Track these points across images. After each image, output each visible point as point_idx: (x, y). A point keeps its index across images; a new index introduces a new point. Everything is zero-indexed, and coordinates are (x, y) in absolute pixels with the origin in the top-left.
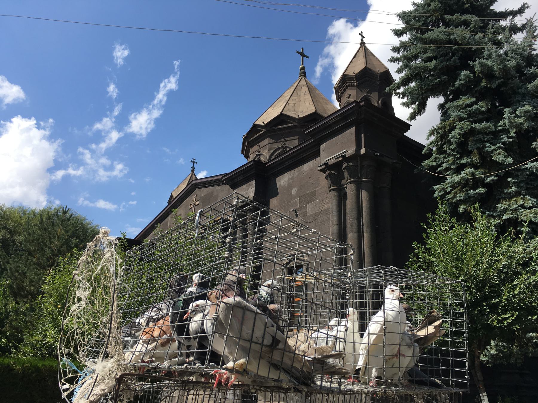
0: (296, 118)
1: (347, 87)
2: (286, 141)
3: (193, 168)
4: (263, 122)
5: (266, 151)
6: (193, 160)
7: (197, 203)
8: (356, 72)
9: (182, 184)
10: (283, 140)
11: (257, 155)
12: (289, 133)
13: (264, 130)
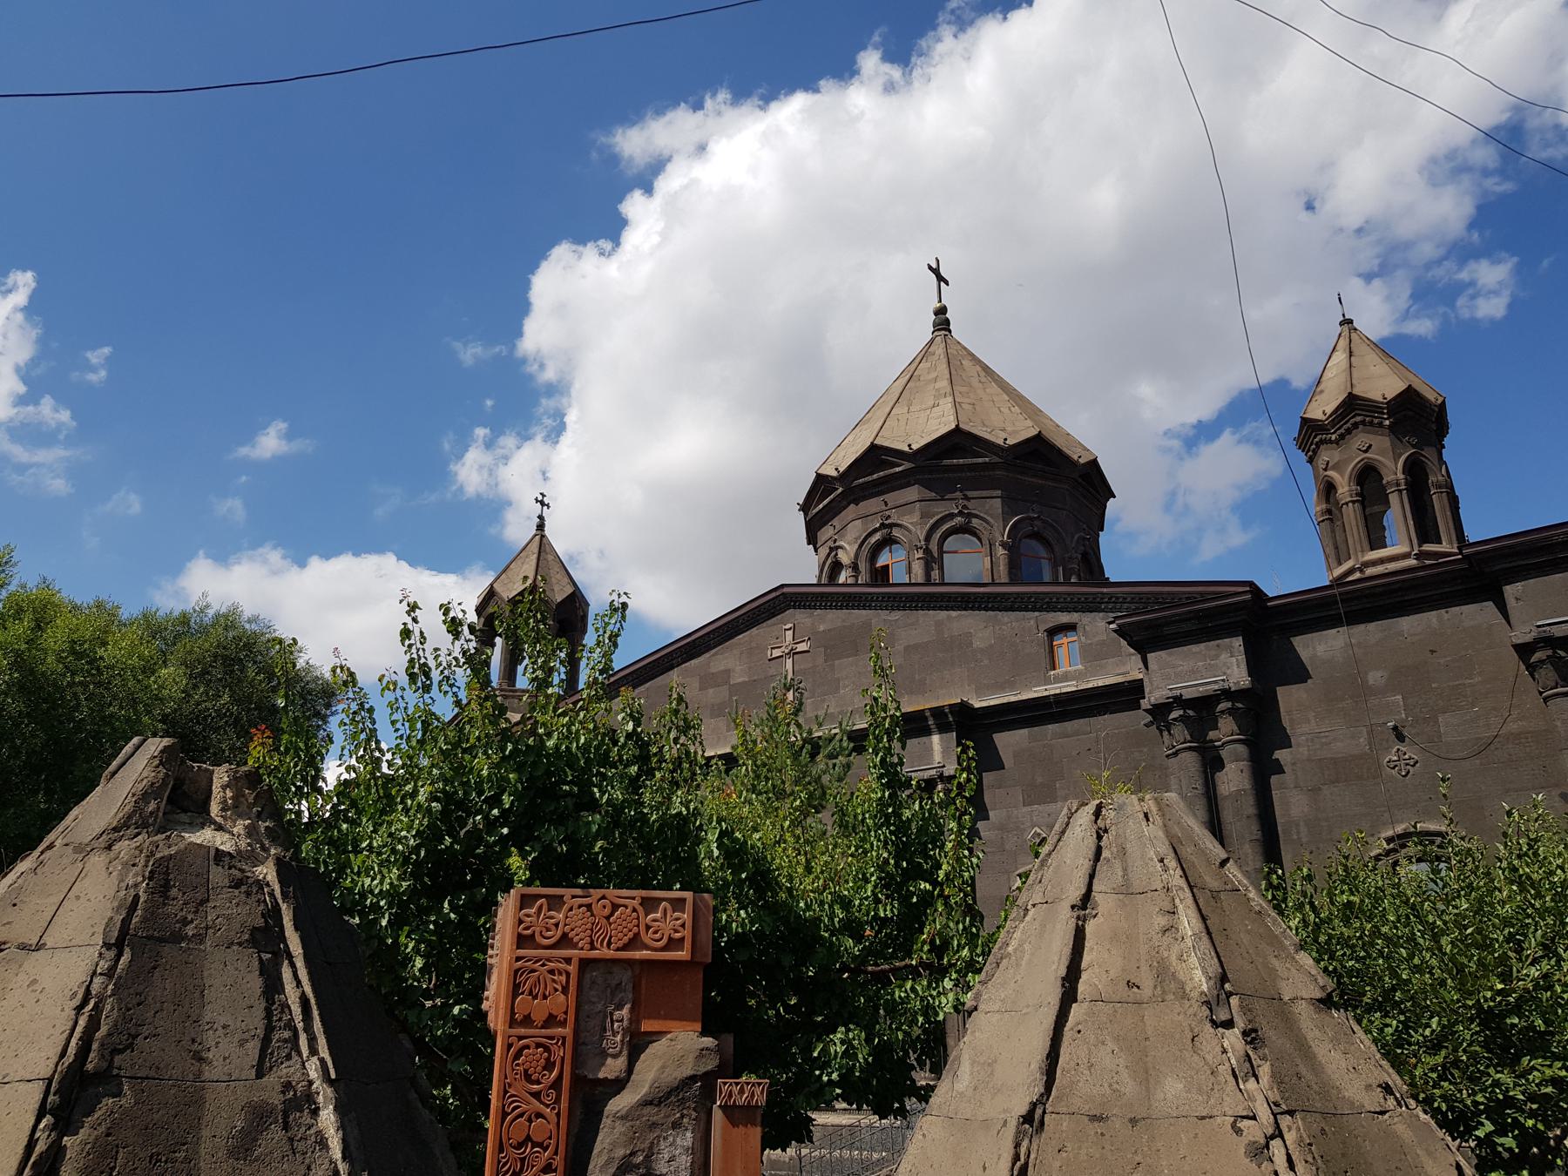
1: (1356, 425)
2: (967, 498)
3: (541, 517)
4: (909, 446)
5: (916, 518)
6: (540, 498)
7: (802, 647)
8: (1390, 396)
9: (519, 562)
11: (882, 524)
12: (979, 479)
13: (906, 465)
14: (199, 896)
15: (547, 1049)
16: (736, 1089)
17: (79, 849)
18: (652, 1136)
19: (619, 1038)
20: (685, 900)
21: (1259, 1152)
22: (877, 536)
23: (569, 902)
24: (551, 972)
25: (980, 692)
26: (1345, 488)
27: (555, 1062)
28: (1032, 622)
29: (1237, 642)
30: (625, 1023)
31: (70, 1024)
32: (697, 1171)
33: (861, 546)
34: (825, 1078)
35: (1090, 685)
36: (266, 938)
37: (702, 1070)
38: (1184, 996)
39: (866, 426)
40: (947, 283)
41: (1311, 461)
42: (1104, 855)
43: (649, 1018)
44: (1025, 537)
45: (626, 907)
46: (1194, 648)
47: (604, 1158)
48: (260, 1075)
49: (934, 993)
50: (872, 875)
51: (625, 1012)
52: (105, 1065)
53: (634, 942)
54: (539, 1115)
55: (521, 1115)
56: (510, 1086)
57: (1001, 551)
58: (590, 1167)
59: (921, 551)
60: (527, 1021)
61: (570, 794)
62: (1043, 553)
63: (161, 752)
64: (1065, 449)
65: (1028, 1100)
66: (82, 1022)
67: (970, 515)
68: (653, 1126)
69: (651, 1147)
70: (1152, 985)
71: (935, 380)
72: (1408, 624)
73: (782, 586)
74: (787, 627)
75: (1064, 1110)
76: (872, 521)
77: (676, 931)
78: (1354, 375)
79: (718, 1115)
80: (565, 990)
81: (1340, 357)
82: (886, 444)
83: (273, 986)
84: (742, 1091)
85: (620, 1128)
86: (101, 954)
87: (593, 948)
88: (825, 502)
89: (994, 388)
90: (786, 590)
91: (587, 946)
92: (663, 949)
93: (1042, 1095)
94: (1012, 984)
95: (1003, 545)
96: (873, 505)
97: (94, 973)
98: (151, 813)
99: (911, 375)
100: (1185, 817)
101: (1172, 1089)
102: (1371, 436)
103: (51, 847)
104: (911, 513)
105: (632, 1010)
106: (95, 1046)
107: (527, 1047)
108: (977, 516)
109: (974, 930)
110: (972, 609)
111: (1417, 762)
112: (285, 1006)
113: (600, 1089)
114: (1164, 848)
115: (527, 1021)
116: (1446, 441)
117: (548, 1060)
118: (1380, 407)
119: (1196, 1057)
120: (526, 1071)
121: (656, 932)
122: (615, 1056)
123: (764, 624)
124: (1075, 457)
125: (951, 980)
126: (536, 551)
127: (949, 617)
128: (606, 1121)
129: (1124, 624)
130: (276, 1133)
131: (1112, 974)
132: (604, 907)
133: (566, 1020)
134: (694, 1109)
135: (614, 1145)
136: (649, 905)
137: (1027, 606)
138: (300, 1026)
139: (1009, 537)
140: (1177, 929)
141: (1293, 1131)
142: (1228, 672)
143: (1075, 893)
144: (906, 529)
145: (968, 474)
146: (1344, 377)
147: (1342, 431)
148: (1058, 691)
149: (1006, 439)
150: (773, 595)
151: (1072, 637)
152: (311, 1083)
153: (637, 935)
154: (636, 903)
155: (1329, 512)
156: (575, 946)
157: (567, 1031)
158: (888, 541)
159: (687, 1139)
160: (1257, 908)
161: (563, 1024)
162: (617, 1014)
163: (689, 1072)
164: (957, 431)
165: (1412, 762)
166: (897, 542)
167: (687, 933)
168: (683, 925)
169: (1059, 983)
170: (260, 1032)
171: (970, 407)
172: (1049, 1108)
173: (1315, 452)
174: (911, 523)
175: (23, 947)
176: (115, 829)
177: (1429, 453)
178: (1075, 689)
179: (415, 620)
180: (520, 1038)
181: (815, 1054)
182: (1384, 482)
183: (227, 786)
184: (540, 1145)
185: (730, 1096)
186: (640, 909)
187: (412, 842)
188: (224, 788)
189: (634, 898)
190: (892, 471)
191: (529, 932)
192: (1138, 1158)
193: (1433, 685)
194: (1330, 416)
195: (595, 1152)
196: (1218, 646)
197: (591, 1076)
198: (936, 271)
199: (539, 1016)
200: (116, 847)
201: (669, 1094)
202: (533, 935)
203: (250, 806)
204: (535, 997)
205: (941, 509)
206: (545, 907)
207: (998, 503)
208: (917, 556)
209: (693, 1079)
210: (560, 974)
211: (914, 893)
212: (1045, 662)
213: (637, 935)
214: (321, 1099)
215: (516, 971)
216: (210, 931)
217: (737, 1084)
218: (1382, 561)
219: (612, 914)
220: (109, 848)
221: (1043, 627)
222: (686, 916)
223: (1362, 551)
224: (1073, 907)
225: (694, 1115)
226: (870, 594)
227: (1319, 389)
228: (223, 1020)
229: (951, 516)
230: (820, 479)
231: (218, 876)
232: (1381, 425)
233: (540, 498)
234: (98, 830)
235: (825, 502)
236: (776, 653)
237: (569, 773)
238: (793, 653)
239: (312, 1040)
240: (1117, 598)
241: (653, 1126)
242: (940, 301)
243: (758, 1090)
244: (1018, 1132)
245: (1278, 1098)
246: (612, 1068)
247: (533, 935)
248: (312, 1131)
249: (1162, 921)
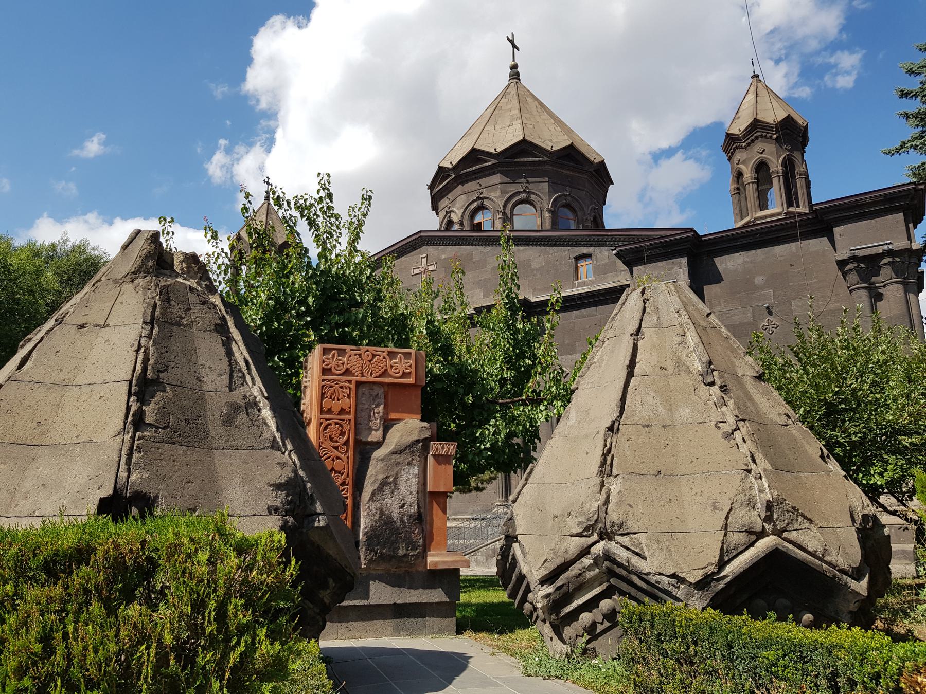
0: (548, 151)
1: (757, 138)
2: (528, 182)
4: (495, 149)
5: (498, 194)
7: (432, 268)
10: (523, 180)
11: (478, 197)
12: (535, 170)
13: (493, 161)
14: (186, 306)
15: (341, 425)
16: (440, 447)
17: (116, 281)
18: (397, 469)
19: (378, 421)
20: (410, 353)
21: (729, 436)
22: (475, 205)
23: (349, 353)
24: (341, 387)
25: (535, 292)
26: (748, 175)
27: (345, 432)
28: (566, 252)
29: (684, 260)
30: (381, 414)
31: (135, 357)
32: (420, 486)
33: (465, 210)
34: (482, 447)
35: (598, 288)
36: (221, 328)
37: (423, 437)
38: (689, 371)
39: (468, 138)
40: (518, 50)
41: (730, 159)
42: (647, 311)
43: (393, 412)
44: (562, 207)
45: (380, 356)
46: (660, 264)
47: (373, 479)
48: (231, 391)
49: (535, 413)
50: (500, 356)
51: (381, 408)
52: (156, 377)
53: (385, 374)
54: (338, 458)
55: (329, 458)
56: (322, 443)
57: (547, 215)
58: (365, 484)
59: (501, 214)
60: (329, 411)
61: (344, 299)
62: (570, 215)
63: (151, 236)
64: (586, 154)
65: (610, 420)
66: (141, 357)
67: (530, 193)
68: (398, 464)
69: (397, 474)
70: (673, 367)
71: (511, 110)
72: (780, 251)
73: (420, 232)
74: (423, 256)
75: (630, 423)
76: (472, 196)
77: (407, 369)
78: (758, 108)
79: (430, 459)
80: (349, 396)
81: (751, 97)
82: (481, 148)
83: (229, 353)
84: (443, 448)
85: (380, 464)
86: (142, 328)
87: (363, 376)
88: (444, 184)
89: (545, 116)
90: (422, 234)
91: (360, 375)
92: (400, 377)
93: (618, 417)
94: (597, 375)
95: (549, 211)
96: (472, 185)
97: (141, 336)
98: (151, 267)
99: (496, 106)
100: (689, 294)
101: (684, 412)
102: (764, 144)
103: (99, 280)
104: (495, 190)
105: (384, 408)
106: (149, 368)
107: (330, 424)
108: (534, 193)
109: (559, 378)
110: (532, 245)
111: (778, 326)
112: (236, 363)
113: (369, 446)
114: (679, 306)
115: (329, 411)
116: (806, 149)
117: (341, 431)
118: (771, 127)
119: (696, 398)
120: (330, 436)
121: (396, 369)
122: (377, 430)
123: (409, 255)
124: (592, 159)
125: (544, 405)
126: (265, 212)
127: (519, 250)
128: (372, 462)
129: (621, 251)
130: (243, 416)
131: (652, 364)
132: (368, 356)
133: (350, 411)
134: (419, 457)
135: (377, 473)
136: (392, 355)
137: (563, 244)
138: (246, 372)
139: (552, 206)
140: (686, 343)
141: (744, 428)
142: (678, 277)
143: (633, 328)
144: (492, 200)
145: (530, 168)
146: (752, 109)
147: (749, 141)
148: (579, 292)
149: (552, 147)
150: (415, 237)
151: (589, 261)
152: (255, 397)
153: (386, 370)
154: (385, 354)
155: (738, 189)
156: (353, 375)
157: (351, 417)
158: (481, 208)
159: (416, 470)
160: (725, 336)
161: (349, 413)
162: (376, 410)
163: (416, 438)
164: (524, 141)
165: (775, 326)
166: (486, 209)
167: (413, 370)
168: (410, 366)
169: (625, 368)
170: (228, 371)
171: (531, 127)
172: (622, 422)
173: (732, 154)
174: (495, 197)
175: (97, 326)
176: (134, 273)
177: (797, 154)
178: (589, 290)
179: (250, 202)
180: (327, 420)
181: (478, 435)
182: (771, 171)
183: (183, 261)
184: (339, 472)
185: (437, 450)
186: (387, 357)
187: (258, 322)
188: (181, 262)
189: (384, 352)
190: (485, 165)
191: (328, 367)
192: (667, 442)
193: (790, 284)
194: (743, 132)
195: (368, 476)
196: (673, 263)
197: (364, 440)
198: (512, 42)
199: (336, 409)
200: (136, 281)
201: (406, 448)
202: (330, 369)
203: (196, 273)
204: (334, 400)
205: (514, 188)
206: (336, 355)
207: (546, 186)
208: (498, 217)
209: (418, 441)
210: (346, 388)
211: (523, 366)
212: (573, 276)
213: (386, 370)
214: (261, 404)
215: (323, 386)
216: (194, 324)
217: (441, 444)
218: (766, 217)
219: (372, 360)
220: (132, 281)
221: (573, 256)
222: (412, 362)
223: (755, 211)
224: (631, 335)
225: (419, 459)
226: (472, 236)
227: (737, 117)
228: (208, 364)
229: (519, 193)
230: (441, 169)
231: (192, 298)
232: (771, 138)
233: (266, 180)
234: (124, 273)
235: (444, 184)
236: (416, 271)
237: (344, 287)
238: (426, 271)
239: (253, 379)
240: (616, 239)
241: (398, 464)
242: (514, 61)
243: (451, 447)
244: (605, 435)
245: (738, 413)
246: (375, 436)
247: (330, 369)
248: (260, 418)
249: (679, 339)
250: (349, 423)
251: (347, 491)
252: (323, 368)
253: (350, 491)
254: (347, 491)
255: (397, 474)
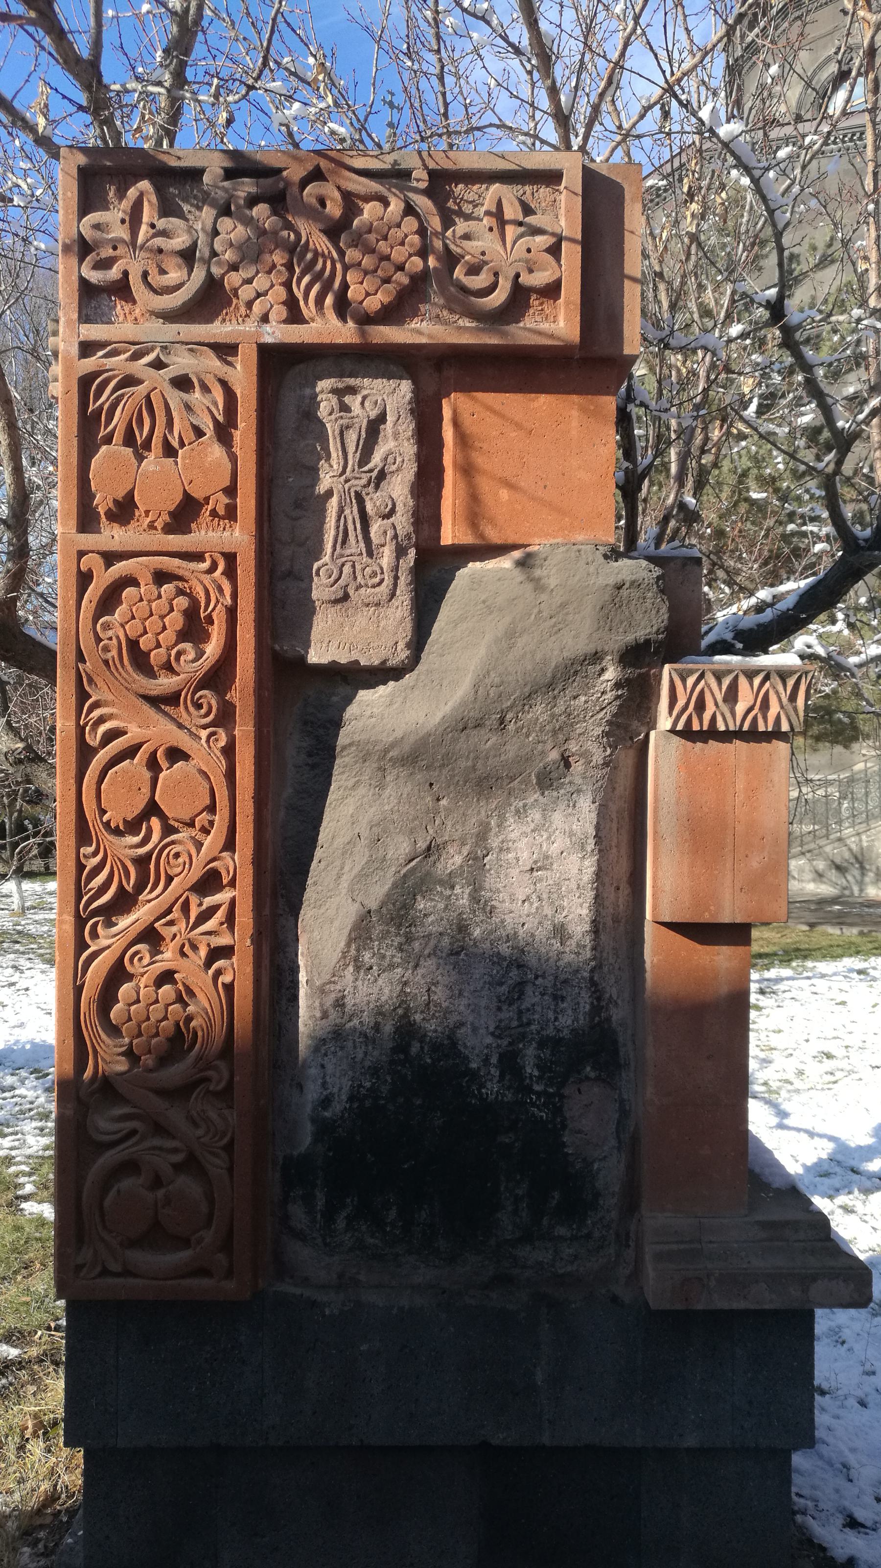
16: (716, 691)
24: (182, 383)
54: (176, 754)
55: (130, 752)
91: (279, 312)
107: (130, 581)
185: (700, 706)
250: (231, 573)
251: (230, 919)
252: (84, 284)
253: (245, 918)
254: (230, 919)
255: (482, 836)
